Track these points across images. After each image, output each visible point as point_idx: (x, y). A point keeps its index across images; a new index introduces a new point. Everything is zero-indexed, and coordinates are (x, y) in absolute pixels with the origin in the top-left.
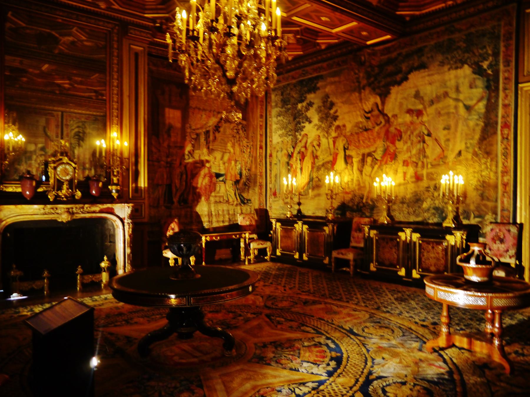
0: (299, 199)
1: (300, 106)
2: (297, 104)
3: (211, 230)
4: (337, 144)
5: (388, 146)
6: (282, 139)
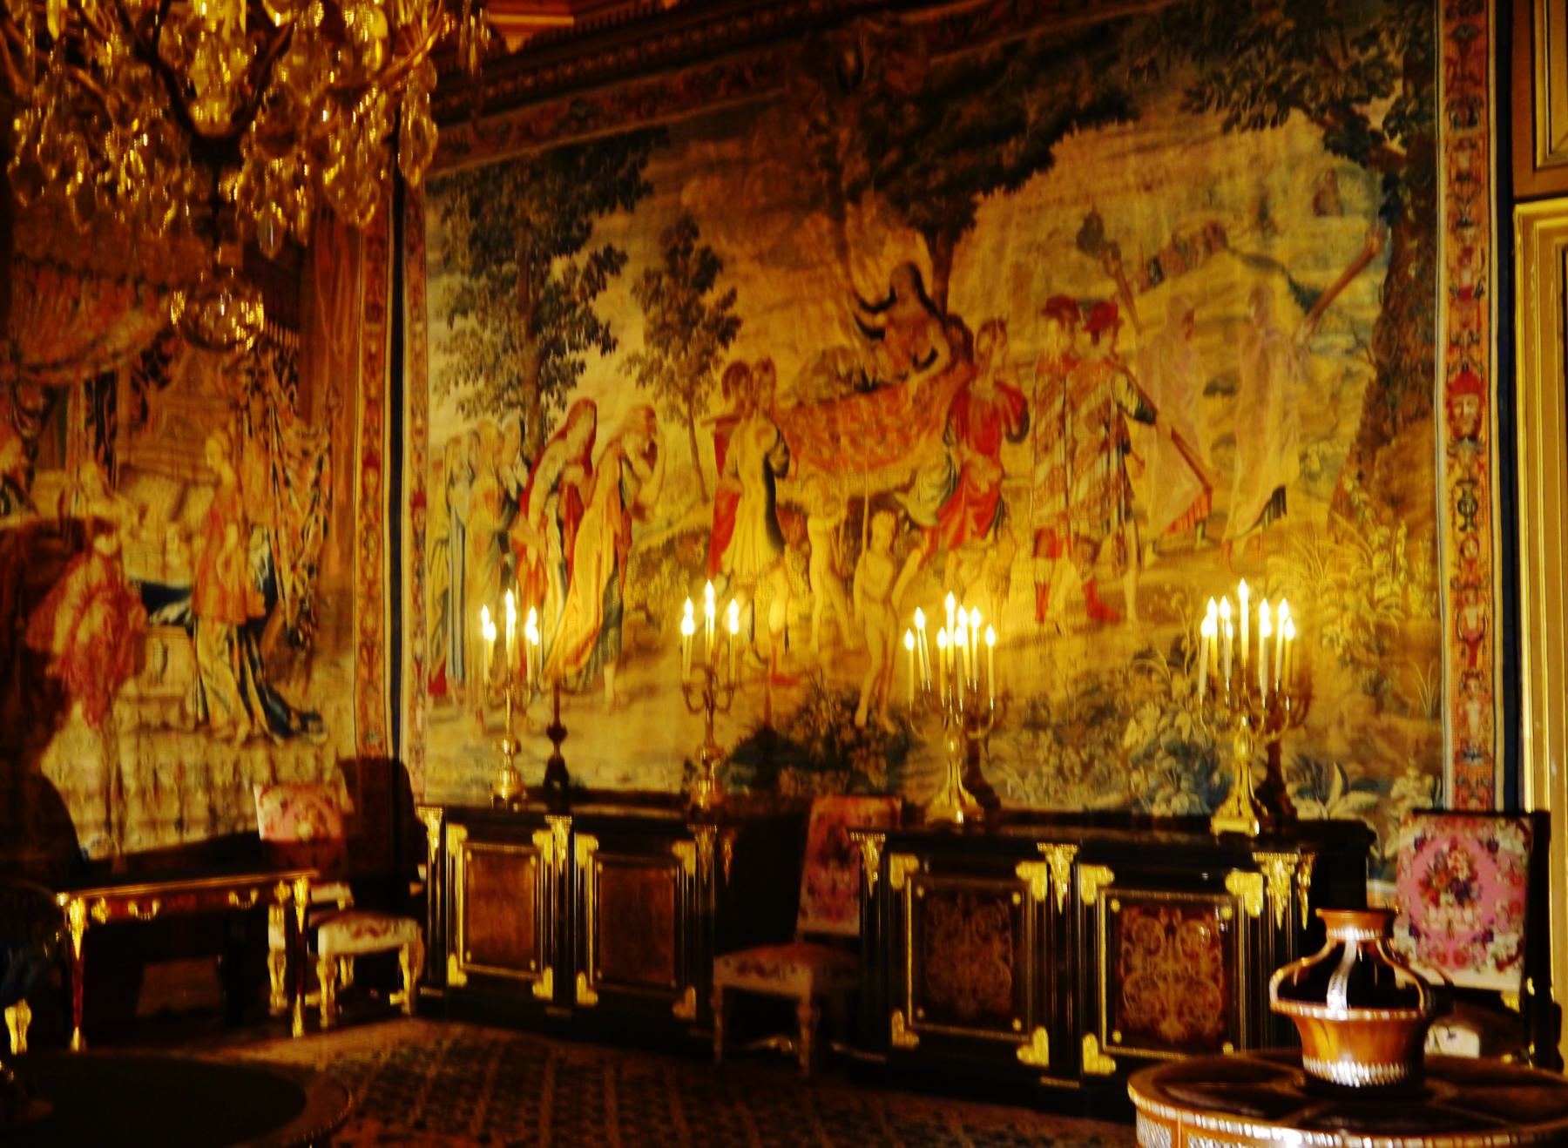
0: (557, 711)
1: (558, 267)
2: (548, 260)
3: (117, 867)
4: (732, 452)
5: (965, 467)
6: (473, 424)
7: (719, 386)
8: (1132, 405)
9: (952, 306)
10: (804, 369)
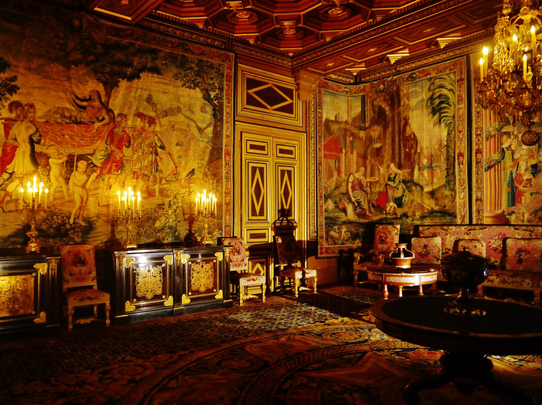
4: (14, 131)
5: (112, 152)
7: (7, 108)
9: (110, 106)
10: (49, 111)
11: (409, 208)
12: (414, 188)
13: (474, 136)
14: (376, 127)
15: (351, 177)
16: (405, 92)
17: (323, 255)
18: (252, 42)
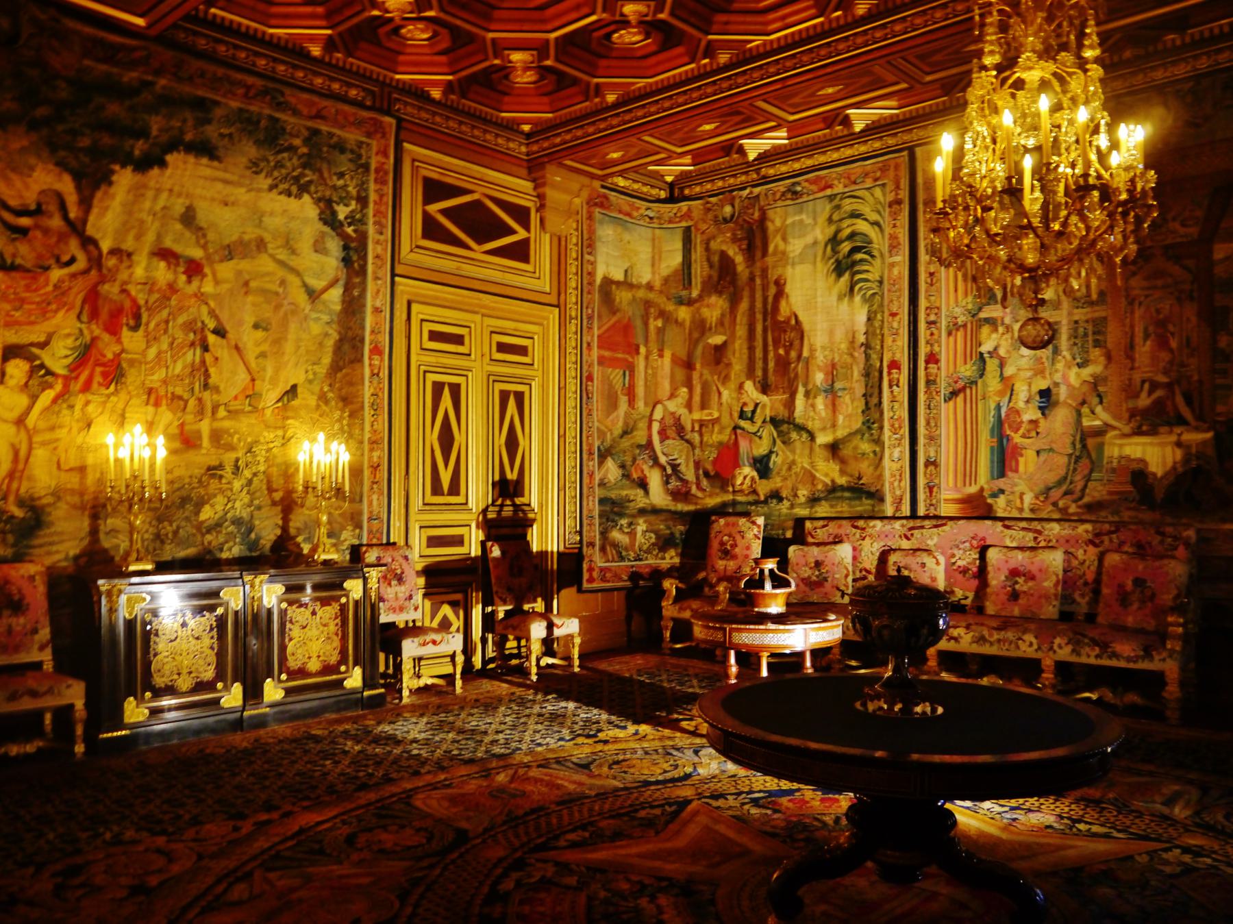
5: (94, 339)
8: (211, 325)
9: (90, 230)
11: (785, 479)
12: (794, 435)
13: (922, 326)
14: (713, 299)
15: (659, 408)
16: (778, 223)
17: (595, 585)
18: (436, 94)
